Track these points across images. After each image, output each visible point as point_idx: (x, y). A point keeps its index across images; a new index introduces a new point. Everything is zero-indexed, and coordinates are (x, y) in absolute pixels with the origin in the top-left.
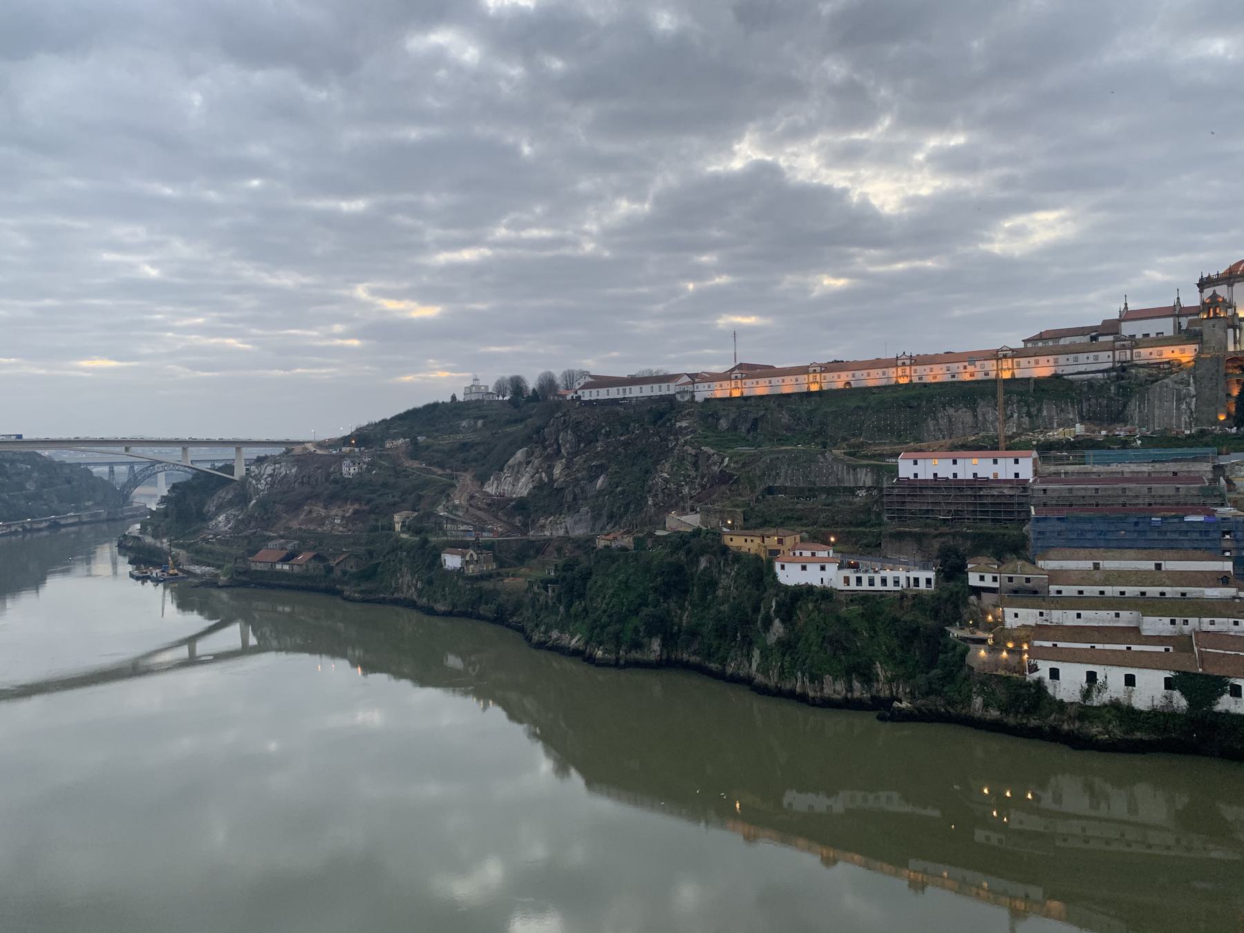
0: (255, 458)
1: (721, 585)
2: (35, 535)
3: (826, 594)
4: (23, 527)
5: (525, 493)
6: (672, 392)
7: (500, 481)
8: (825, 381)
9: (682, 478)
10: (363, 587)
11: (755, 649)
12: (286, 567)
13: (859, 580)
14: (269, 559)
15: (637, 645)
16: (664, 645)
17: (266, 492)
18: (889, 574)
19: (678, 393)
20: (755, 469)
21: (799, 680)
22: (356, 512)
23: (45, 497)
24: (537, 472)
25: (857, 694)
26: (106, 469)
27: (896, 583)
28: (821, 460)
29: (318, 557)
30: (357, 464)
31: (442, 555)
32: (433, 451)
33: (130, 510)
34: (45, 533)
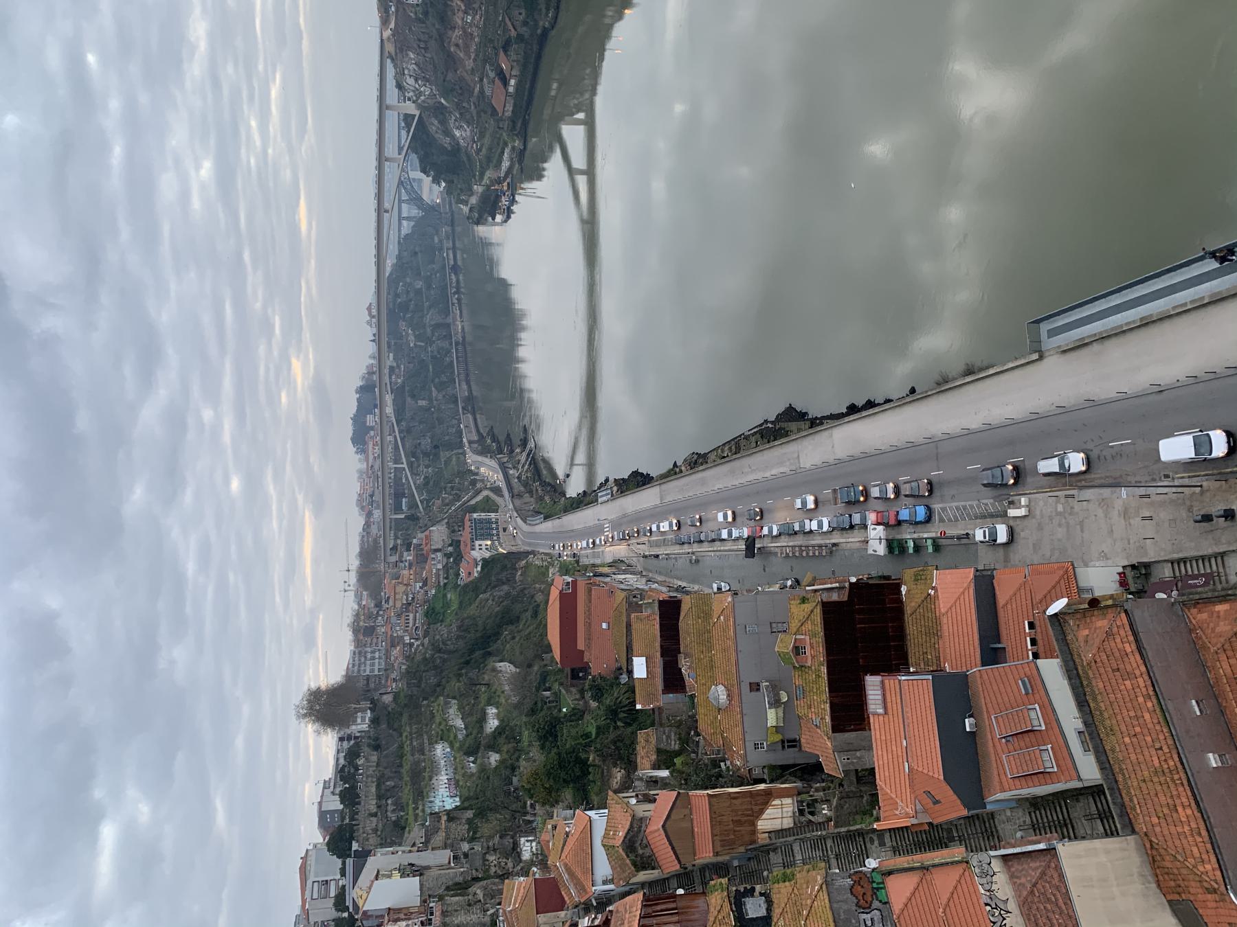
0: (397, 90)
2: (462, 285)
4: (455, 293)
10: (543, 7)
12: (513, 82)
14: (503, 98)
17: (434, 87)
23: (429, 274)
26: (405, 223)
29: (506, 47)
33: (444, 207)
34: (461, 278)
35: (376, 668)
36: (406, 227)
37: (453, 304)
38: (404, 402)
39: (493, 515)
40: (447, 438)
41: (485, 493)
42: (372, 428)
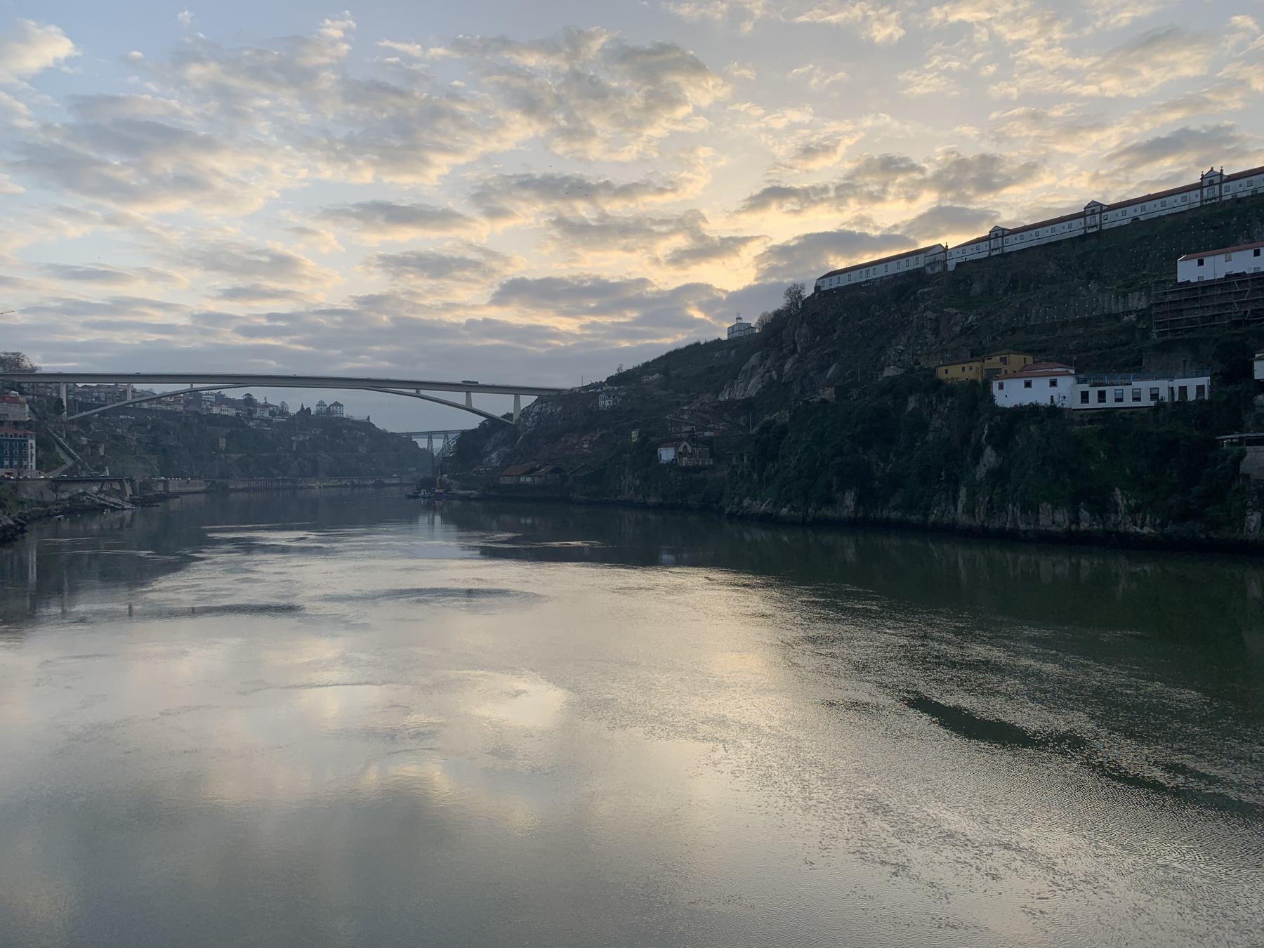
1: (931, 428)
3: (1053, 411)
5: (753, 393)
6: (921, 265)
7: (733, 388)
8: (1106, 221)
9: (919, 348)
11: (962, 487)
12: (529, 479)
13: (1102, 396)
15: (829, 501)
16: (859, 501)
17: (532, 429)
18: (1145, 386)
19: (928, 265)
20: (1000, 316)
21: (1010, 513)
22: (602, 436)
23: (374, 460)
24: (768, 372)
25: (1084, 526)
27: (1154, 396)
28: (1083, 293)
30: (612, 397)
31: (659, 449)
32: (683, 379)
37: (339, 480)
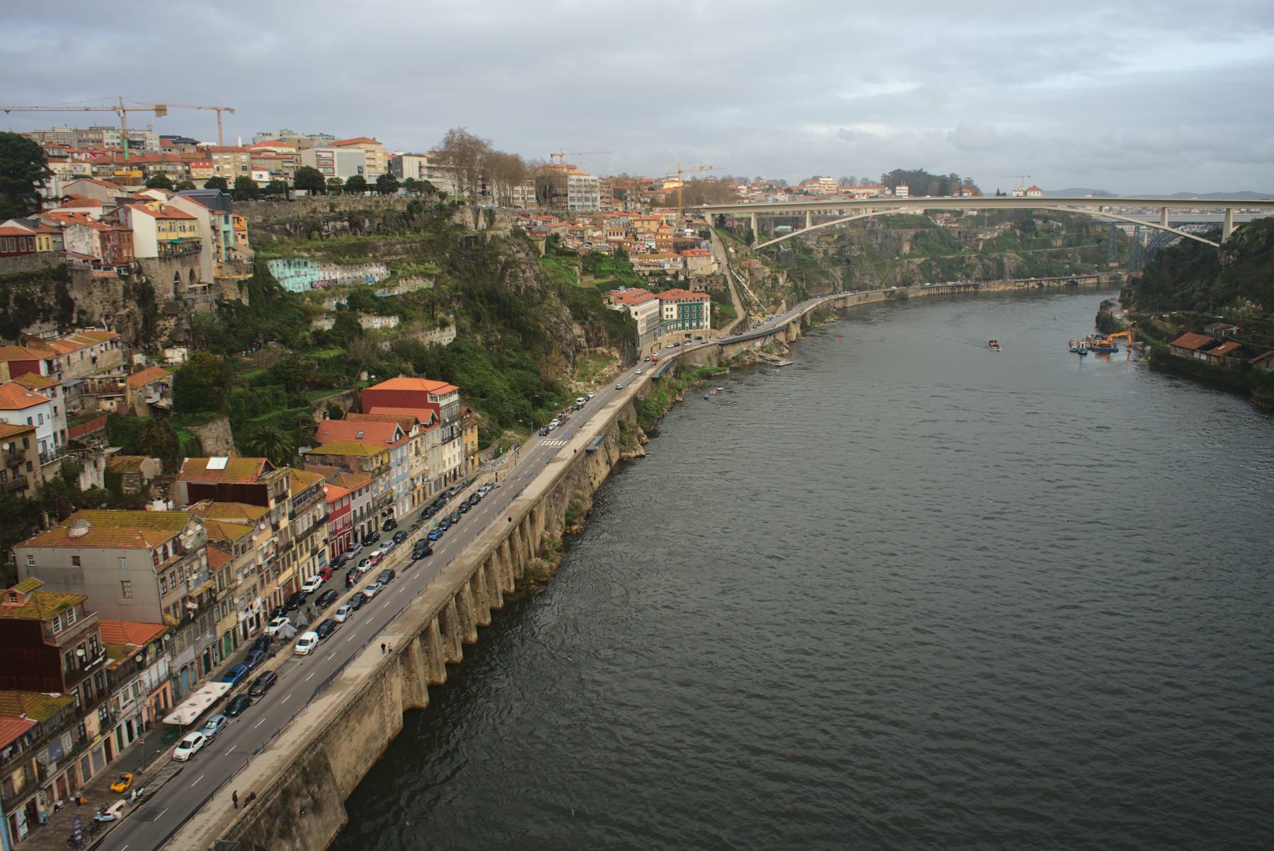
12: (1204, 357)
35: (576, 203)
36: (1129, 231)
38: (910, 227)
39: (708, 323)
40: (857, 274)
41: (741, 314)
42: (894, 192)
